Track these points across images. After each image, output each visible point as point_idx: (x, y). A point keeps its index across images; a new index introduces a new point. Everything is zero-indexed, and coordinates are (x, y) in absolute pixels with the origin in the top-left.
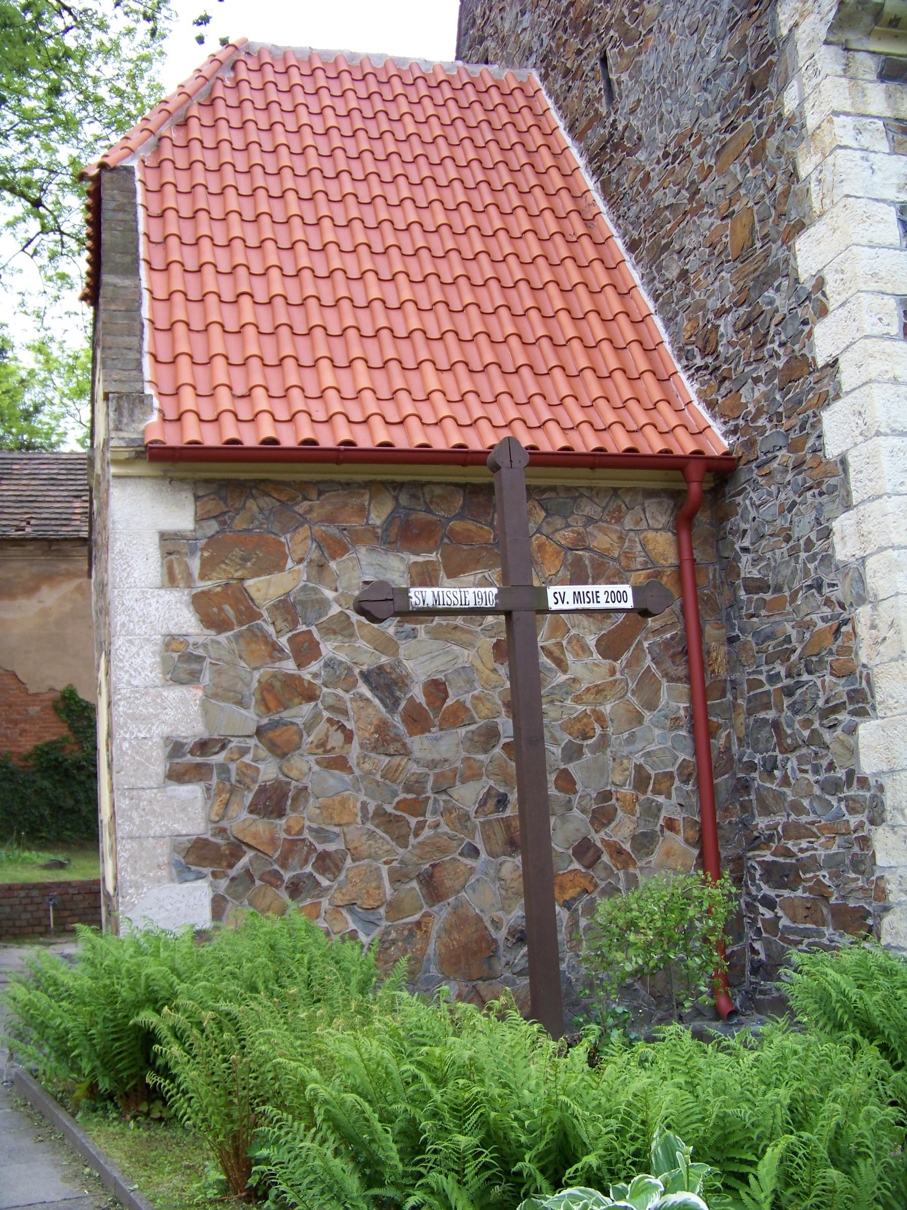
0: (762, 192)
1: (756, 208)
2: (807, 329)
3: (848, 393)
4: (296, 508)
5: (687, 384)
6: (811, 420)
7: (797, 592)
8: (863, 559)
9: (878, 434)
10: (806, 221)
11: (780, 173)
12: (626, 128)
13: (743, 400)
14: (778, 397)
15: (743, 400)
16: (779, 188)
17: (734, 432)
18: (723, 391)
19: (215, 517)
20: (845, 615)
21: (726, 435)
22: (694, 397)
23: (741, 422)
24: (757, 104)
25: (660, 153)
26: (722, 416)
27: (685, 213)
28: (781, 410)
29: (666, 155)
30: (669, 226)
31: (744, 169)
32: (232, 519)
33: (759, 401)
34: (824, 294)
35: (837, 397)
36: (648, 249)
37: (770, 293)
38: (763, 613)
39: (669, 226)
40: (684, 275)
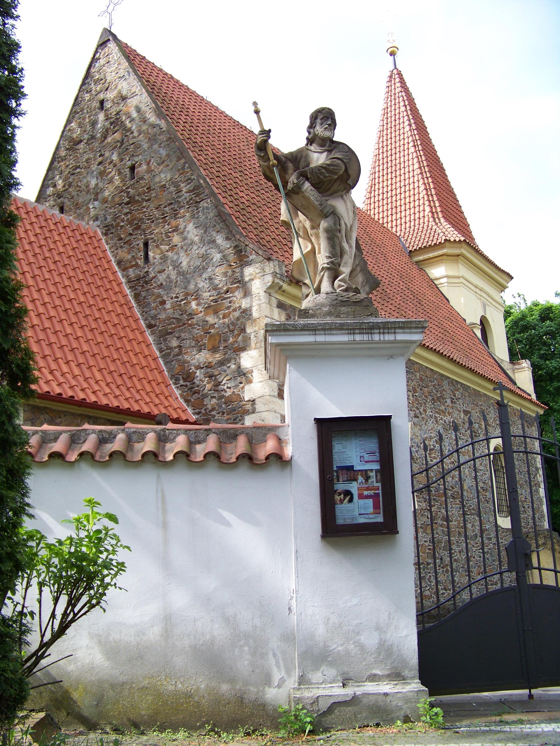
0: (226, 330)
1: (223, 335)
2: (241, 385)
3: (258, 412)
4: (56, 421)
5: (175, 390)
6: (239, 418)
11: (237, 327)
12: (154, 277)
13: (205, 403)
14: (223, 406)
15: (205, 403)
17: (198, 414)
18: (194, 397)
19: (30, 420)
21: (194, 414)
22: (179, 396)
23: (203, 411)
25: (174, 296)
26: (193, 406)
27: (184, 324)
28: (225, 411)
29: (177, 297)
30: (174, 326)
32: (35, 421)
33: (213, 406)
34: (252, 376)
35: (253, 412)
36: (160, 331)
39: (174, 326)
40: (180, 347)
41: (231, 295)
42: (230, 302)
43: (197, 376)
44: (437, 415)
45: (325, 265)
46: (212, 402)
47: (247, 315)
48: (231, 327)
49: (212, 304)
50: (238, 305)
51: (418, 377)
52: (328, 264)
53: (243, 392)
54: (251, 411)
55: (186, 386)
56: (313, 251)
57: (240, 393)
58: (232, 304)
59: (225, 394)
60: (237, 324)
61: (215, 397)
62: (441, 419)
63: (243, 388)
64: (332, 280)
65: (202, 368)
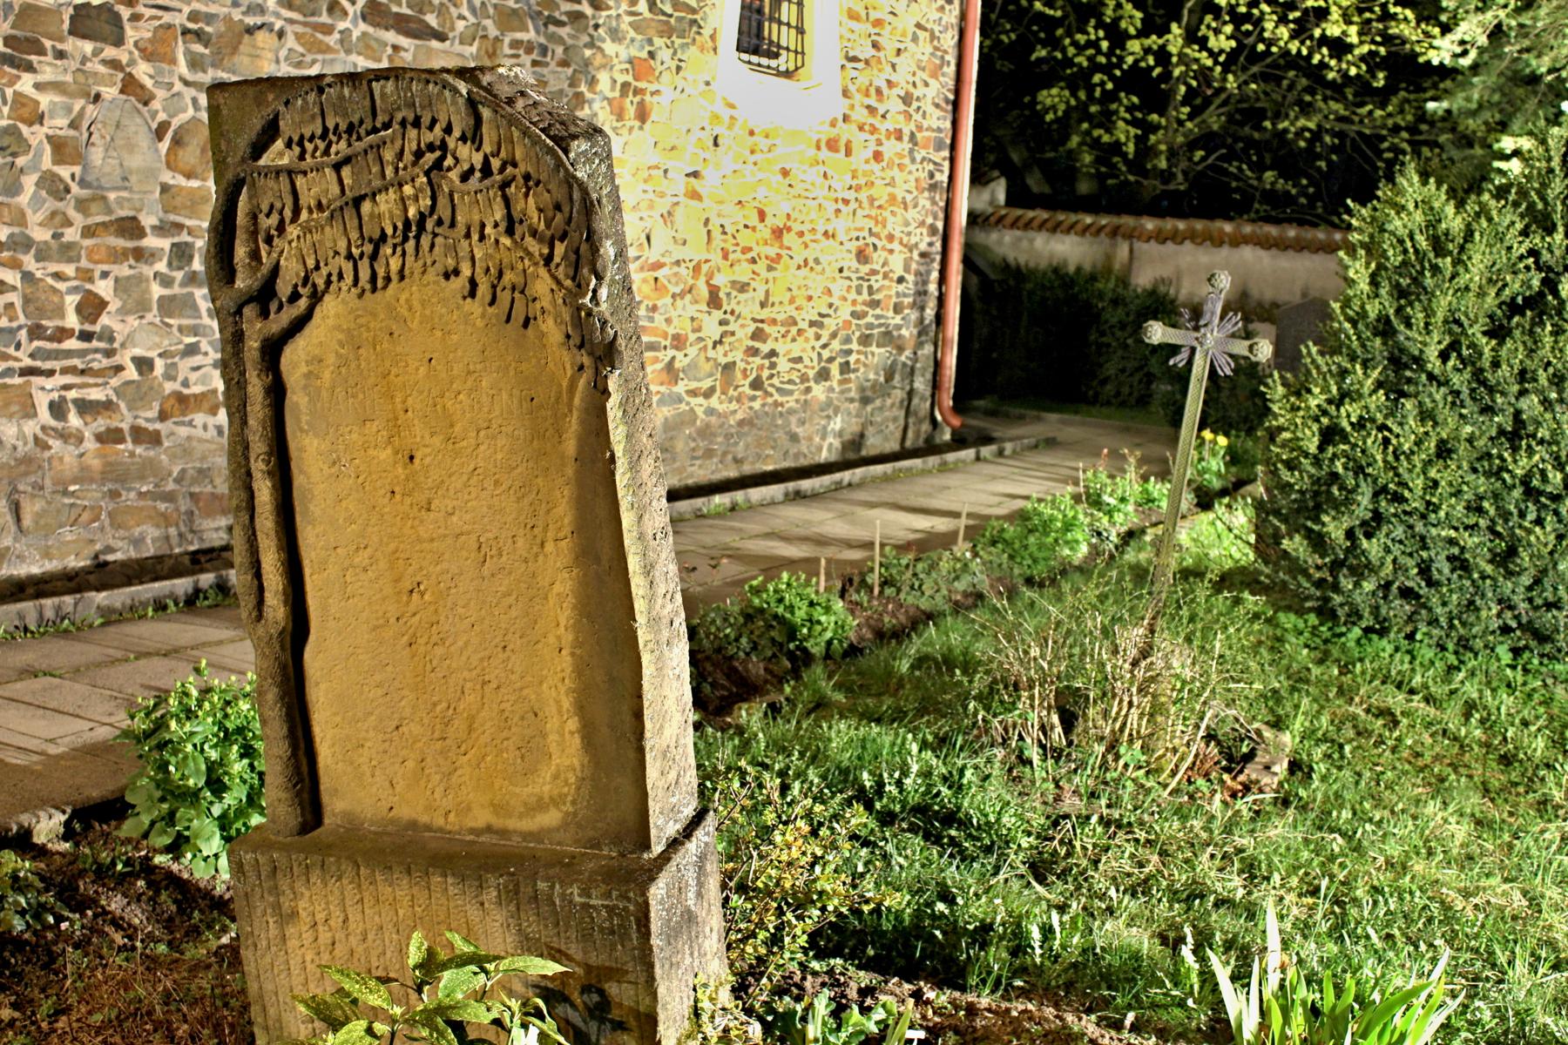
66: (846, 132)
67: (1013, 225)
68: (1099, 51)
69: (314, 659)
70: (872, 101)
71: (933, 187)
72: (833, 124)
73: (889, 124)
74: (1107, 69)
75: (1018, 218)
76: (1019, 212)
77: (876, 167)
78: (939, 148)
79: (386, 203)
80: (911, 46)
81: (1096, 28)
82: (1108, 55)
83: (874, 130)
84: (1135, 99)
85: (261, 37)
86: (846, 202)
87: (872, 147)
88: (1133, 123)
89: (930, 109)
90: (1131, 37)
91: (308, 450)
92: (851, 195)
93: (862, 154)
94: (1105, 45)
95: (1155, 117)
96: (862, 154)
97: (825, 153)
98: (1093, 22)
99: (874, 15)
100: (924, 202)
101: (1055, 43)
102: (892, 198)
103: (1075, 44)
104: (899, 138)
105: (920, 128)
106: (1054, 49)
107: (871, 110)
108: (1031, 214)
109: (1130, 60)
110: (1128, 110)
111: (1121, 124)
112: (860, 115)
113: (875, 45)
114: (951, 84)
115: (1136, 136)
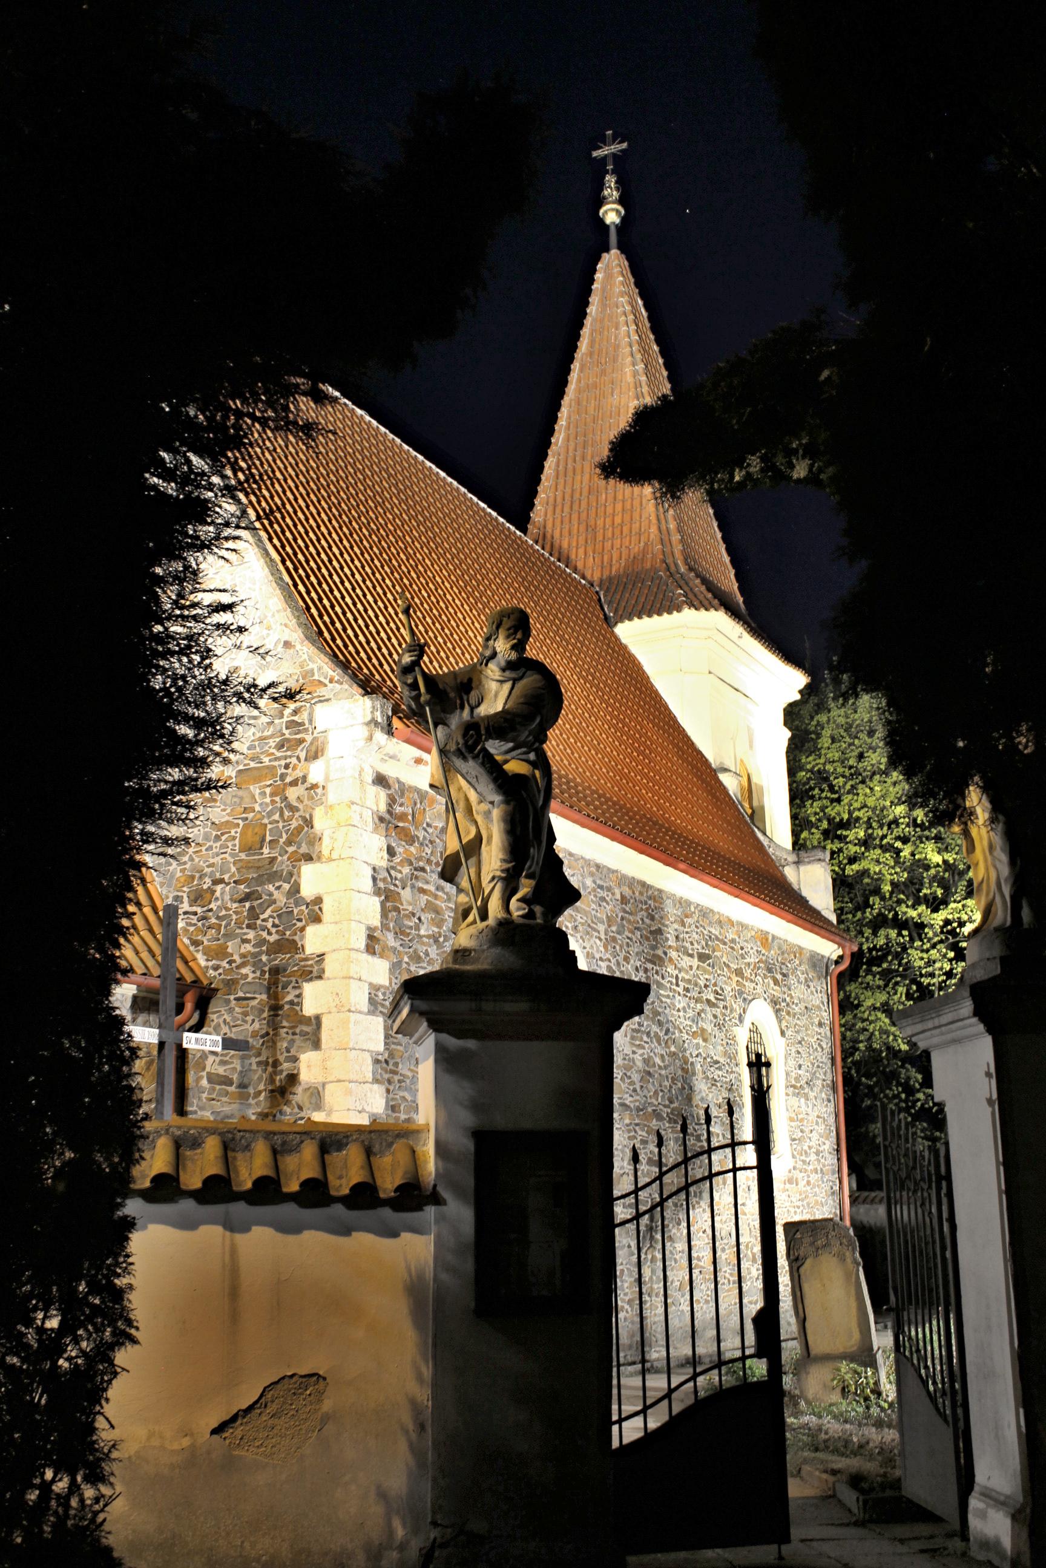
2: (299, 924)
7: (260, 1092)
8: (324, 1085)
9: (349, 1011)
10: (314, 856)
13: (230, 950)
16: (294, 824)
20: (302, 1115)
24: (286, 758)
31: (263, 794)
34: (320, 909)
35: (320, 977)
37: (271, 888)
38: (224, 1099)
41: (289, 753)
42: (287, 767)
43: (217, 899)
44: (649, 966)
45: (498, 873)
46: (243, 951)
47: (317, 794)
48: (287, 814)
49: (252, 764)
50: (301, 775)
51: (618, 897)
52: (502, 871)
53: (302, 938)
54: (315, 974)
55: (195, 914)
56: (479, 838)
57: (296, 938)
58: (289, 771)
59: (268, 938)
60: (298, 810)
61: (247, 941)
62: (657, 973)
63: (303, 929)
64: (507, 894)
65: (228, 884)
66: (797, 1174)
67: (864, 1202)
68: (901, 1100)
69: (807, 1324)
70: (803, 1158)
71: (833, 1193)
72: (790, 1171)
73: (811, 1167)
74: (907, 1110)
75: (867, 1197)
76: (866, 1194)
77: (808, 1188)
78: (833, 1174)
79: (819, 1242)
80: (816, 1127)
81: (897, 1086)
82: (906, 1101)
83: (806, 1171)
84: (925, 1125)
85: (625, 1176)
86: (798, 1207)
87: (806, 1179)
88: (925, 1138)
89: (827, 1155)
90: (918, 1091)
91: (806, 1287)
92: (800, 1203)
93: (802, 1183)
94: (903, 1096)
95: (938, 1134)
96: (802, 1183)
97: (788, 1186)
98: (894, 1083)
99: (800, 1117)
100: (830, 1202)
101: (875, 1097)
102: (816, 1202)
103: (886, 1096)
104: (816, 1173)
105: (824, 1166)
106: (875, 1100)
107: (804, 1162)
108: (873, 1194)
109: (919, 1104)
110: (922, 1131)
111: (920, 1140)
112: (800, 1165)
113: (802, 1131)
114: (835, 1140)
115: (929, 1147)
